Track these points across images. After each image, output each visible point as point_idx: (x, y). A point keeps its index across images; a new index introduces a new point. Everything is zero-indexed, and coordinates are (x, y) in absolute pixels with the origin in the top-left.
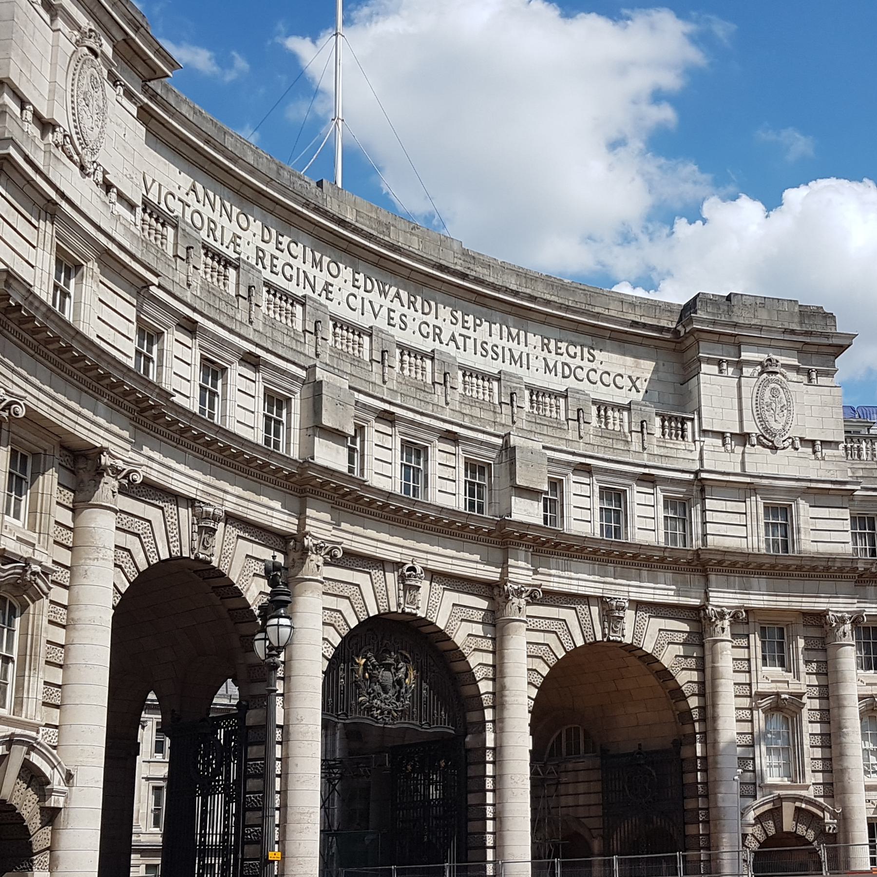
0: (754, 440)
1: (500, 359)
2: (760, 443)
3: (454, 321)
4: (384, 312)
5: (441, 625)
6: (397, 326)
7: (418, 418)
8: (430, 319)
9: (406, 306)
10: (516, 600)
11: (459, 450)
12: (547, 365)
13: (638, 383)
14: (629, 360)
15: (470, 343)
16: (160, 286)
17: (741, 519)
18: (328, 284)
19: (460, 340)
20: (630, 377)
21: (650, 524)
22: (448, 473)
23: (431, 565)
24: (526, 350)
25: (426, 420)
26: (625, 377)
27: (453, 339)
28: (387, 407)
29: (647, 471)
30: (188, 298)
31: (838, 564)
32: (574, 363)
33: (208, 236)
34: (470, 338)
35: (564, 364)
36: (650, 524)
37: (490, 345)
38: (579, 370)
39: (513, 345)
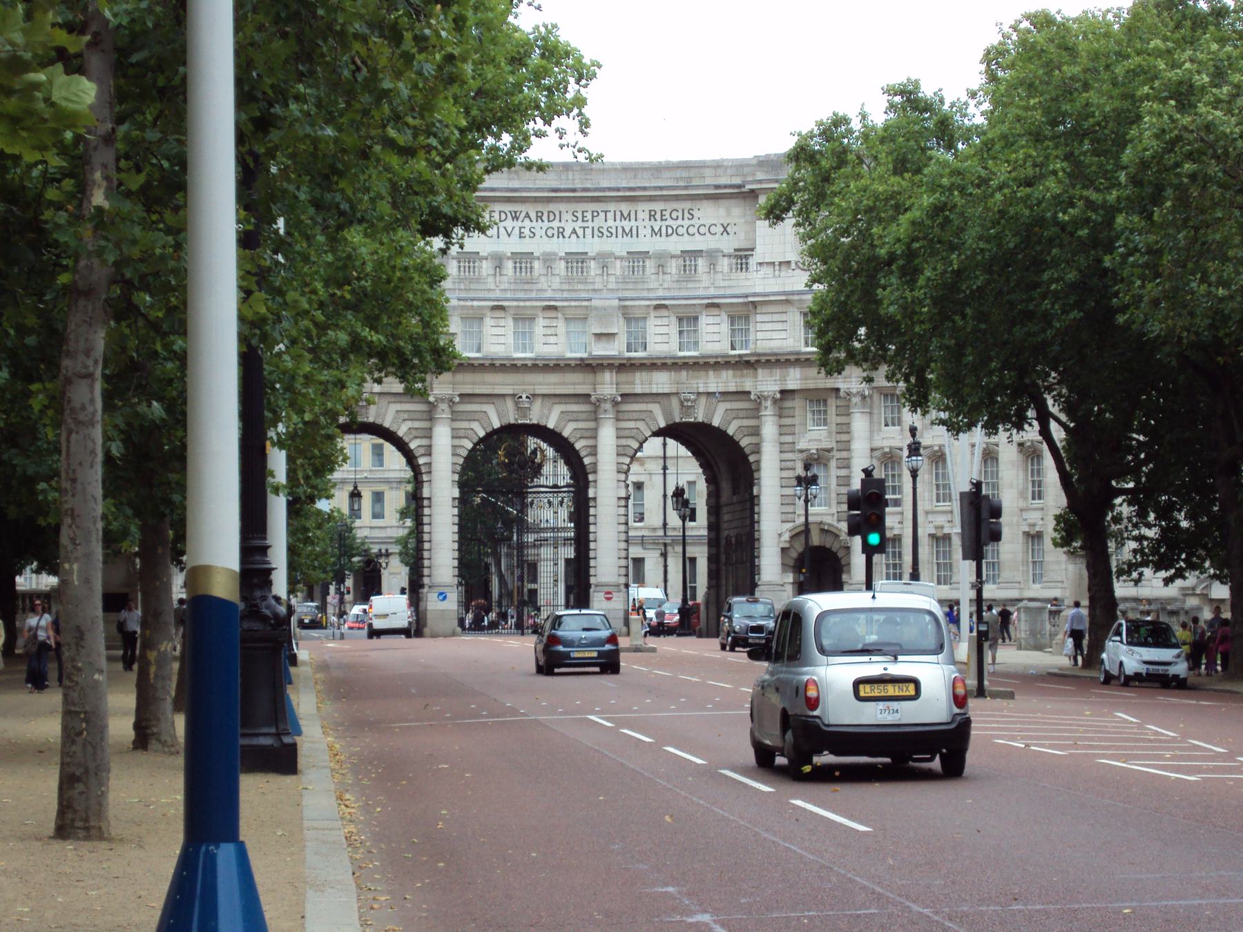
0: (793, 266)
2: (799, 268)
4: (517, 231)
5: (551, 425)
7: (522, 304)
8: (556, 224)
9: (534, 220)
11: (560, 315)
12: (653, 229)
13: (728, 229)
14: (722, 211)
15: (588, 231)
19: (580, 232)
21: (716, 337)
22: (549, 331)
23: (537, 392)
25: (528, 304)
27: (574, 231)
28: (496, 303)
29: (710, 301)
32: (674, 224)
36: (716, 337)
38: (680, 228)
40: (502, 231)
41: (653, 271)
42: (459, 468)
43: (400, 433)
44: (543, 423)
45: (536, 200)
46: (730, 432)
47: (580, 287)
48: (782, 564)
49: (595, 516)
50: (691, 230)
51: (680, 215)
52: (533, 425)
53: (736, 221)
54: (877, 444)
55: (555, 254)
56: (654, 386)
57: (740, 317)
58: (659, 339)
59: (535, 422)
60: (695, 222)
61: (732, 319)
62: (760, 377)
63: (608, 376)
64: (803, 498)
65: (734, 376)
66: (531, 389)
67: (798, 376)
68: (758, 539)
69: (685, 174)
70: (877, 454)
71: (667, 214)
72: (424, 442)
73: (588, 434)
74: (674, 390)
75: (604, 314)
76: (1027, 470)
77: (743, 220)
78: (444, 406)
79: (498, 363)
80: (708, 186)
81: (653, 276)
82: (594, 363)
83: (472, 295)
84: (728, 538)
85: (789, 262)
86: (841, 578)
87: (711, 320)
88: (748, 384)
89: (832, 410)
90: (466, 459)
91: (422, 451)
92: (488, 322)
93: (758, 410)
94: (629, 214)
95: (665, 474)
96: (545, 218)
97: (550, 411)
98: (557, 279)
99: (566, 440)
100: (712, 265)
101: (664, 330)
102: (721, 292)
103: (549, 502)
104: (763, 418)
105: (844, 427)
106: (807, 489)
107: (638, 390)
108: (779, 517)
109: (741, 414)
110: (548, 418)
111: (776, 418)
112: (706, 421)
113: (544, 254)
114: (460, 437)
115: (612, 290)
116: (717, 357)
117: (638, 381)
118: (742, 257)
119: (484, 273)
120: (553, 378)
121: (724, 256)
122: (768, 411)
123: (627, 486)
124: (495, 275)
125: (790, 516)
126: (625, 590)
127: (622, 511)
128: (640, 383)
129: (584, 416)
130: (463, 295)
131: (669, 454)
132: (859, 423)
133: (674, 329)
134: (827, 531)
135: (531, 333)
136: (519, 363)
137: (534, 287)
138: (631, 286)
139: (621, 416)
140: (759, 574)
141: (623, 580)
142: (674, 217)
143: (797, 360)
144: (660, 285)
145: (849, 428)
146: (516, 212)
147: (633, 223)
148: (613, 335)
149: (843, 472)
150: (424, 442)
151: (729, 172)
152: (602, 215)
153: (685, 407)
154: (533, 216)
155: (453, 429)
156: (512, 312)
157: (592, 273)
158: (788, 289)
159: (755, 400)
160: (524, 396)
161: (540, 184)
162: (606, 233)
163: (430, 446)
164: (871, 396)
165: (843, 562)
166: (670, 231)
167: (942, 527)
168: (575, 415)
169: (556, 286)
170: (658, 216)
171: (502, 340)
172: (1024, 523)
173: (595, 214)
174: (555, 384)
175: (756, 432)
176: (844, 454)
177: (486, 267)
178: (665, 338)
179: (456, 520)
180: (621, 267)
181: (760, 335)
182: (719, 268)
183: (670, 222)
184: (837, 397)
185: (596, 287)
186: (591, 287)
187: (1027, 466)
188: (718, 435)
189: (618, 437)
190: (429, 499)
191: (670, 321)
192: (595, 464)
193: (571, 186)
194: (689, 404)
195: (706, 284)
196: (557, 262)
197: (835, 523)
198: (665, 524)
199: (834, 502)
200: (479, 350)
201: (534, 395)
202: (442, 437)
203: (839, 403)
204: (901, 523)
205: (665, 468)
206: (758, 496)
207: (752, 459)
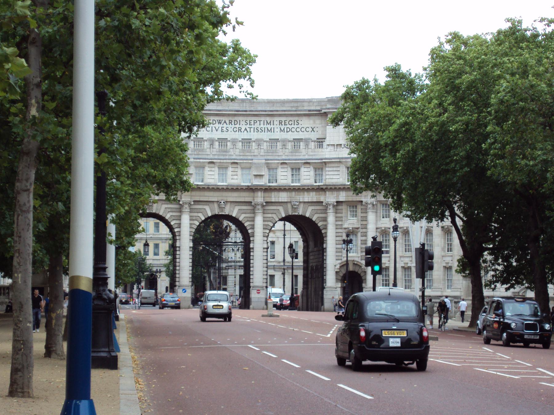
0: (343, 146)
4: (220, 129)
5: (234, 215)
7: (222, 161)
8: (238, 126)
11: (239, 166)
12: (281, 129)
13: (314, 129)
14: (311, 122)
15: (252, 129)
19: (248, 130)
22: (234, 173)
23: (228, 200)
24: (273, 126)
25: (225, 161)
27: (246, 129)
28: (210, 161)
29: (306, 161)
32: (290, 127)
35: (287, 128)
38: (293, 129)
40: (214, 128)
41: (281, 147)
42: (192, 234)
43: (167, 218)
44: (230, 214)
45: (229, 115)
46: (314, 219)
47: (248, 154)
48: (336, 279)
49: (253, 256)
50: (298, 130)
52: (226, 215)
53: (318, 126)
54: (379, 226)
55: (237, 139)
56: (280, 198)
57: (319, 169)
58: (283, 178)
61: (315, 169)
62: (327, 196)
63: (260, 194)
64: (346, 249)
65: (316, 195)
66: (225, 199)
67: (344, 195)
68: (326, 267)
69: (296, 105)
70: (379, 230)
71: (287, 122)
72: (177, 222)
73: (251, 219)
74: (289, 201)
75: (258, 166)
76: (445, 239)
77: (321, 126)
78: (186, 206)
79: (211, 187)
80: (305, 110)
81: (281, 150)
82: (254, 188)
83: (200, 157)
84: (312, 267)
85: (341, 145)
86: (362, 285)
87: (306, 170)
88: (322, 198)
89: (359, 211)
90: (196, 229)
91: (176, 226)
92: (207, 169)
93: (326, 210)
94: (270, 122)
95: (284, 238)
96: (233, 123)
97: (234, 209)
98: (238, 150)
99: (240, 222)
100: (307, 145)
101: (285, 174)
102: (311, 157)
103: (233, 250)
104: (329, 214)
105: (364, 218)
106: (347, 245)
107: (273, 200)
108: (334, 258)
109: (319, 212)
110: (233, 212)
111: (334, 214)
112: (303, 214)
113: (232, 139)
114: (193, 220)
115: (262, 155)
116: (308, 186)
117: (273, 196)
118: (320, 142)
119: (205, 147)
120: (235, 194)
121: (312, 141)
122: (331, 210)
123: (268, 243)
124: (210, 148)
125: (340, 257)
126: (266, 289)
127: (265, 254)
128: (274, 197)
129: (249, 211)
130: (196, 157)
131: (286, 229)
132: (371, 217)
133: (289, 173)
134: (356, 264)
135: (226, 174)
136: (220, 187)
137: (227, 154)
138: (270, 154)
139: (265, 211)
140: (325, 283)
141: (265, 285)
142: (290, 124)
143: (344, 188)
144: (284, 154)
145: (367, 219)
146: (220, 120)
147: (272, 126)
148: (262, 175)
149: (364, 238)
150: (177, 222)
151: (315, 104)
153: (294, 208)
154: (228, 122)
155: (190, 216)
156: (217, 165)
157: (254, 148)
158: (340, 156)
159: (325, 206)
160: (222, 202)
161: (231, 108)
162: (260, 130)
163: (180, 224)
164: (376, 205)
165: (363, 278)
166: (288, 130)
167: (407, 263)
168: (245, 211)
169: (237, 153)
170: (283, 123)
171: (213, 177)
172: (444, 262)
173: (255, 122)
174: (236, 197)
175: (325, 219)
176: (364, 230)
177: (206, 145)
178: (285, 177)
179: (191, 257)
180: (266, 145)
181: (328, 177)
182: (310, 147)
183: (288, 126)
184: (362, 205)
185: (255, 154)
186: (253, 154)
187: (445, 237)
188: (308, 221)
189: (264, 221)
190: (179, 247)
191: (288, 170)
192: (253, 233)
193: (244, 109)
194: (296, 207)
195: (304, 153)
196: (238, 142)
197: (360, 261)
198: (284, 260)
199: (359, 251)
200: (202, 181)
201: (227, 202)
202: (186, 219)
203: (362, 207)
204: (389, 261)
205: (284, 235)
206: (326, 248)
207: (323, 231)
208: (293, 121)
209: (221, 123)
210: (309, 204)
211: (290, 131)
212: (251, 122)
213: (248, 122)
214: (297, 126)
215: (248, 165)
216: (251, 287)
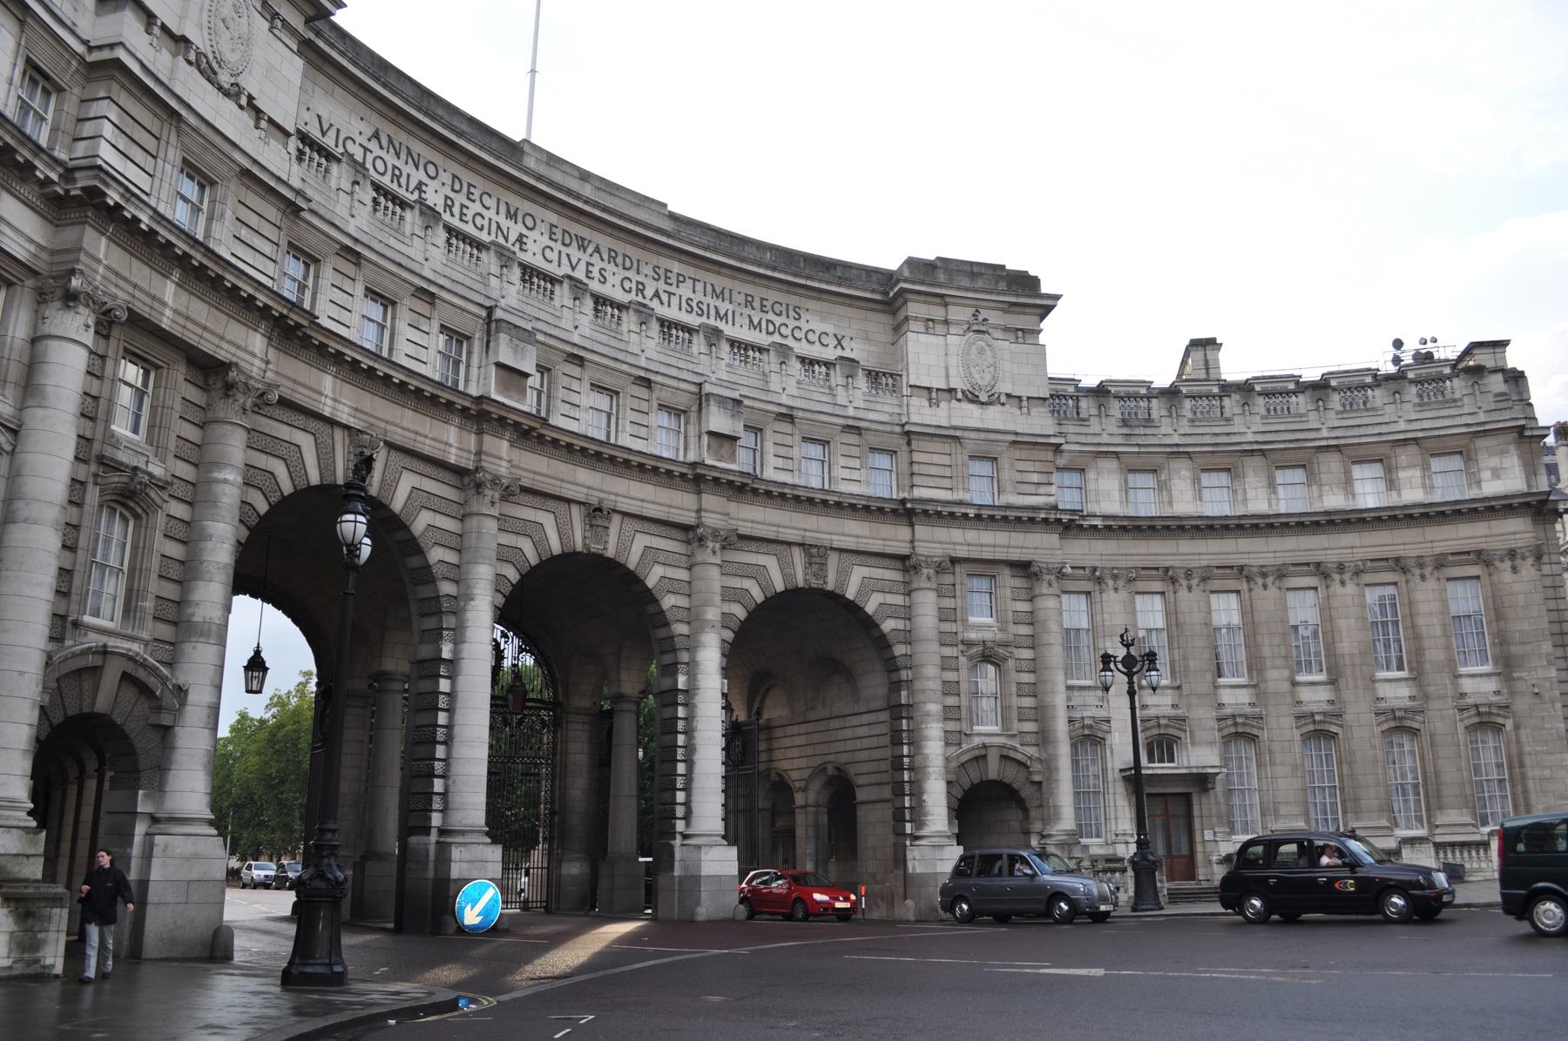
1: (705, 316)
3: (656, 276)
6: (596, 280)
10: (710, 544)
12: (751, 321)
15: (674, 300)
16: (312, 211)
17: (947, 472)
18: (521, 235)
19: (664, 297)
20: (835, 335)
24: (731, 307)
26: (831, 335)
27: (657, 295)
30: (427, 273)
31: (1043, 516)
32: (778, 321)
33: (392, 181)
34: (674, 294)
35: (768, 321)
37: (695, 302)
39: (719, 303)
40: (564, 260)
46: (870, 608)
51: (784, 309)
59: (610, 553)
60: (802, 323)
85: (951, 391)
96: (619, 260)
152: (689, 283)
162: (695, 308)
166: (771, 328)
170: (756, 304)
175: (908, 613)
183: (771, 316)
201: (614, 510)
208: (784, 306)
209: (585, 251)
210: (853, 558)
211: (777, 334)
212: (669, 274)
213: (661, 272)
214: (797, 323)
215: (682, 401)
216: (678, 841)
